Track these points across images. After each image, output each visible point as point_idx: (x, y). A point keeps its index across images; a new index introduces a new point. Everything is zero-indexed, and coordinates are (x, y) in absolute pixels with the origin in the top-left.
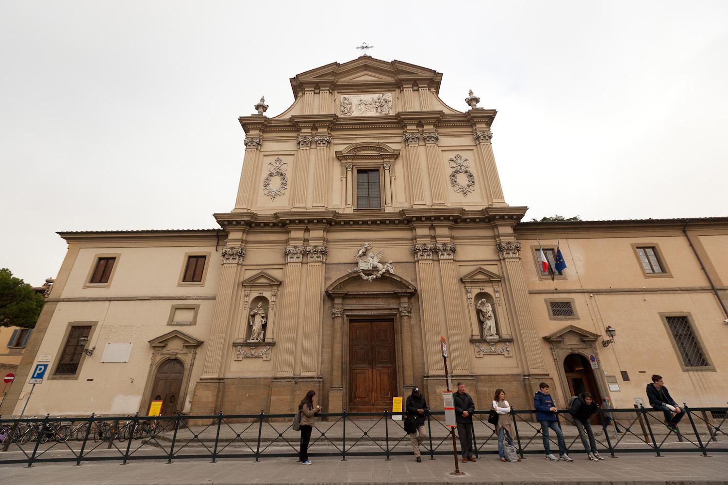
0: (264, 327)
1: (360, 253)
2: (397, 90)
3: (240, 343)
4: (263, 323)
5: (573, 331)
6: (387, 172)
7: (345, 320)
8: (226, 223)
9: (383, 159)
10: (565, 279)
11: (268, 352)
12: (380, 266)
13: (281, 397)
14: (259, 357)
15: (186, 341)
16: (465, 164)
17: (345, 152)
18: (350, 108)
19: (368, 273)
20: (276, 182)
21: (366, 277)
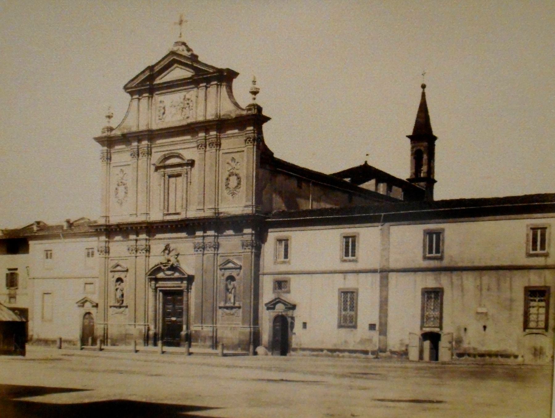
0: (122, 295)
16: (238, 167)
20: (121, 189)
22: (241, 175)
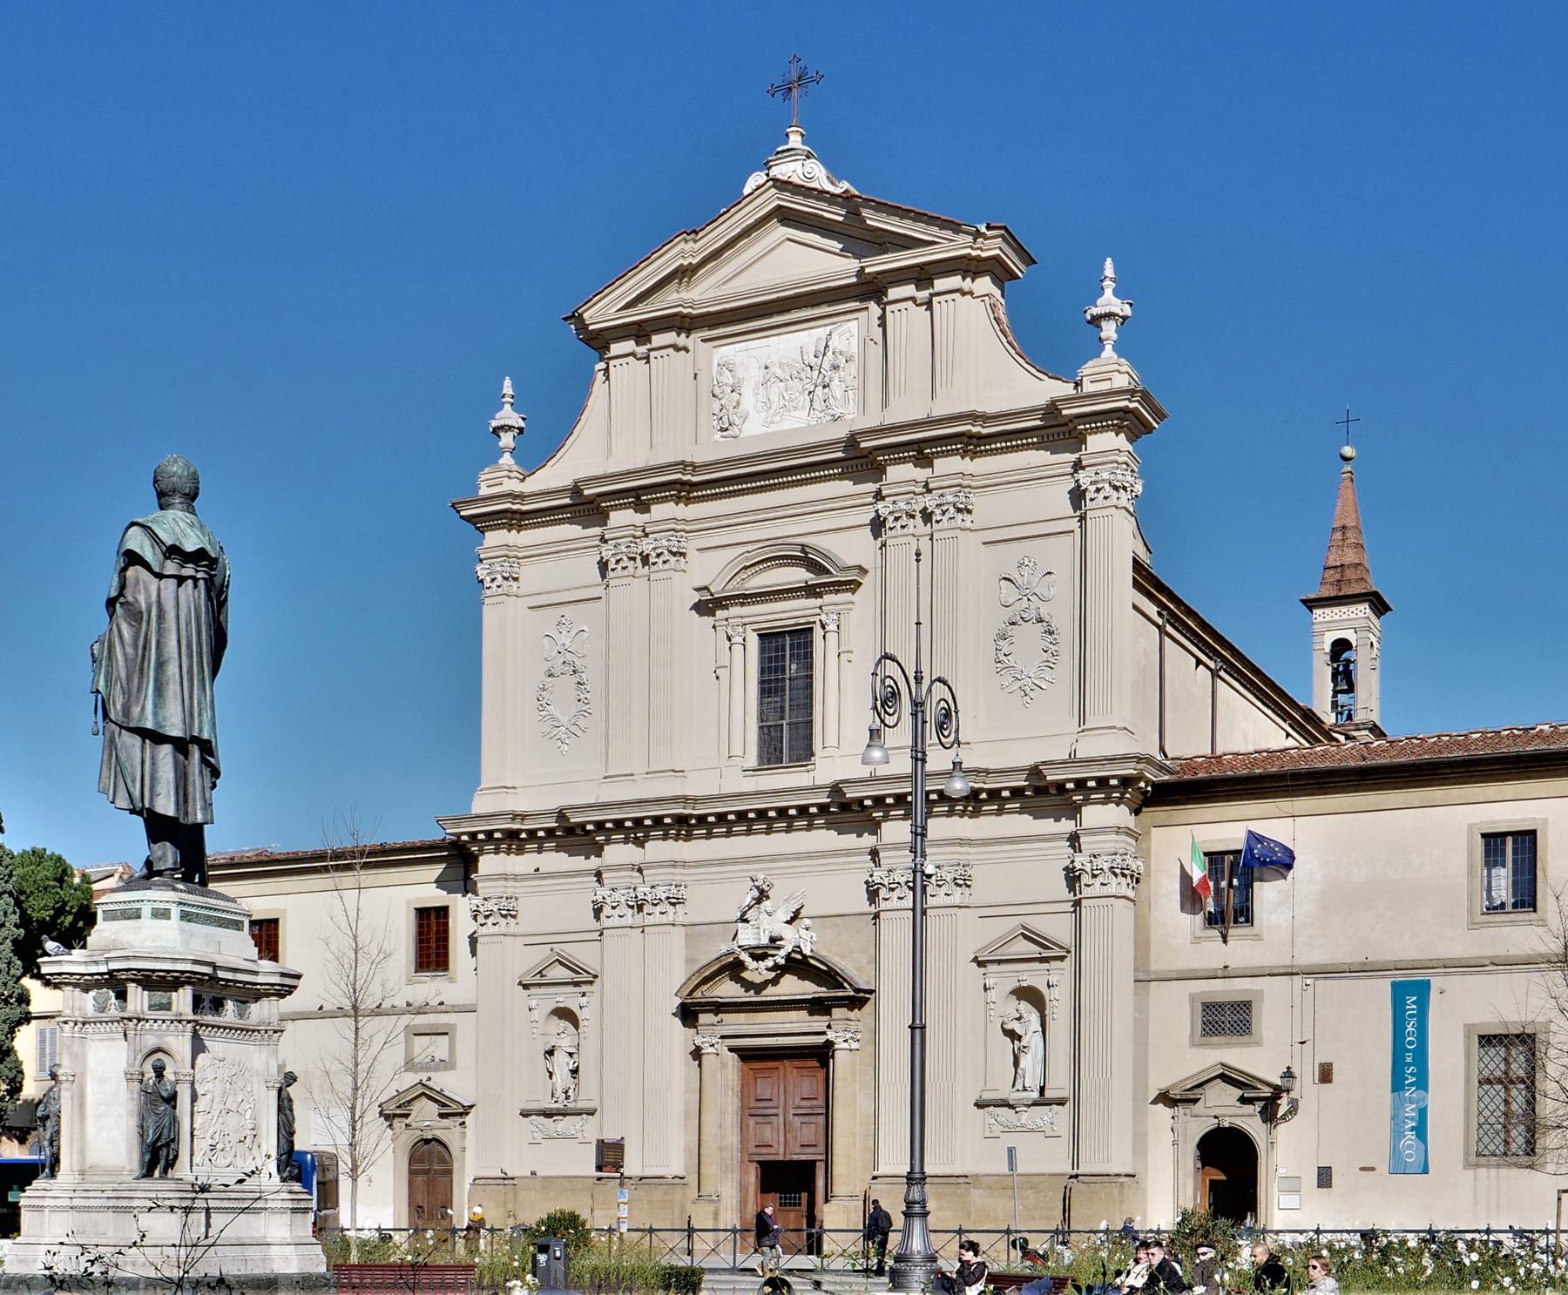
5: (1227, 1077)
6: (832, 637)
9: (820, 595)
10: (1258, 937)
15: (444, 1105)
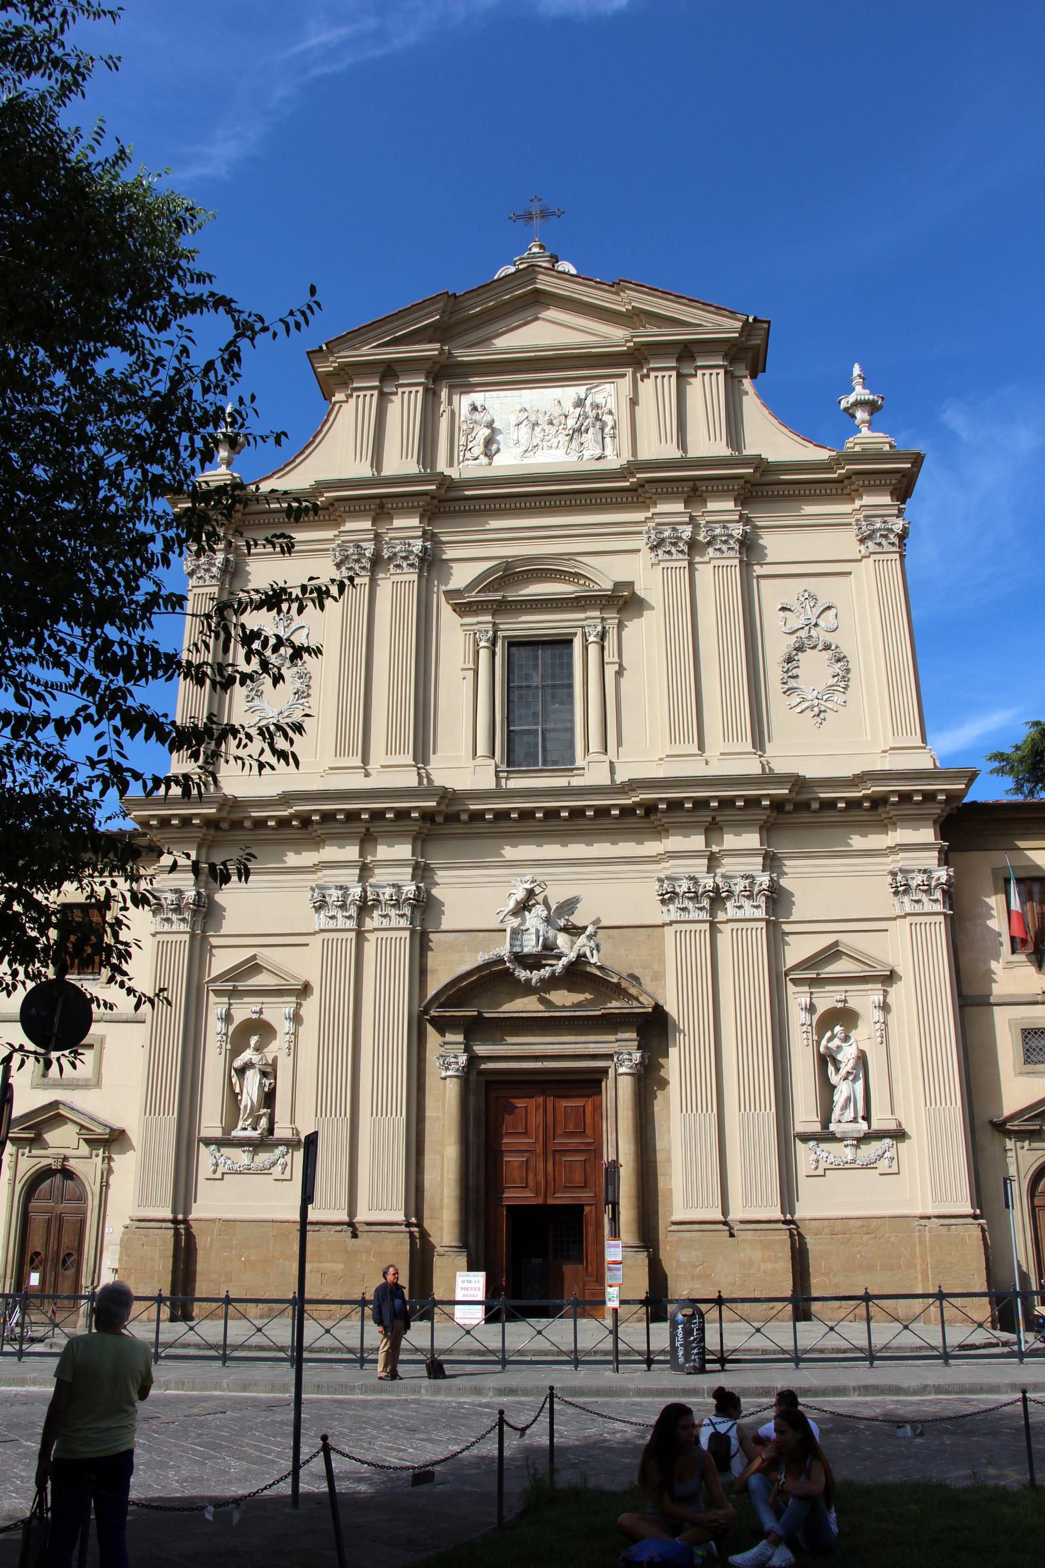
0: (269, 1098)
1: (512, 904)
2: (629, 371)
3: (216, 1139)
4: (266, 1089)
7: (472, 1085)
8: (154, 822)
9: (583, 609)
11: (282, 1160)
12: (562, 940)
13: (322, 1265)
14: (264, 1171)
15: (82, 1127)
17: (473, 597)
18: (489, 442)
19: (532, 962)
21: (523, 974)
22: (845, 650)
